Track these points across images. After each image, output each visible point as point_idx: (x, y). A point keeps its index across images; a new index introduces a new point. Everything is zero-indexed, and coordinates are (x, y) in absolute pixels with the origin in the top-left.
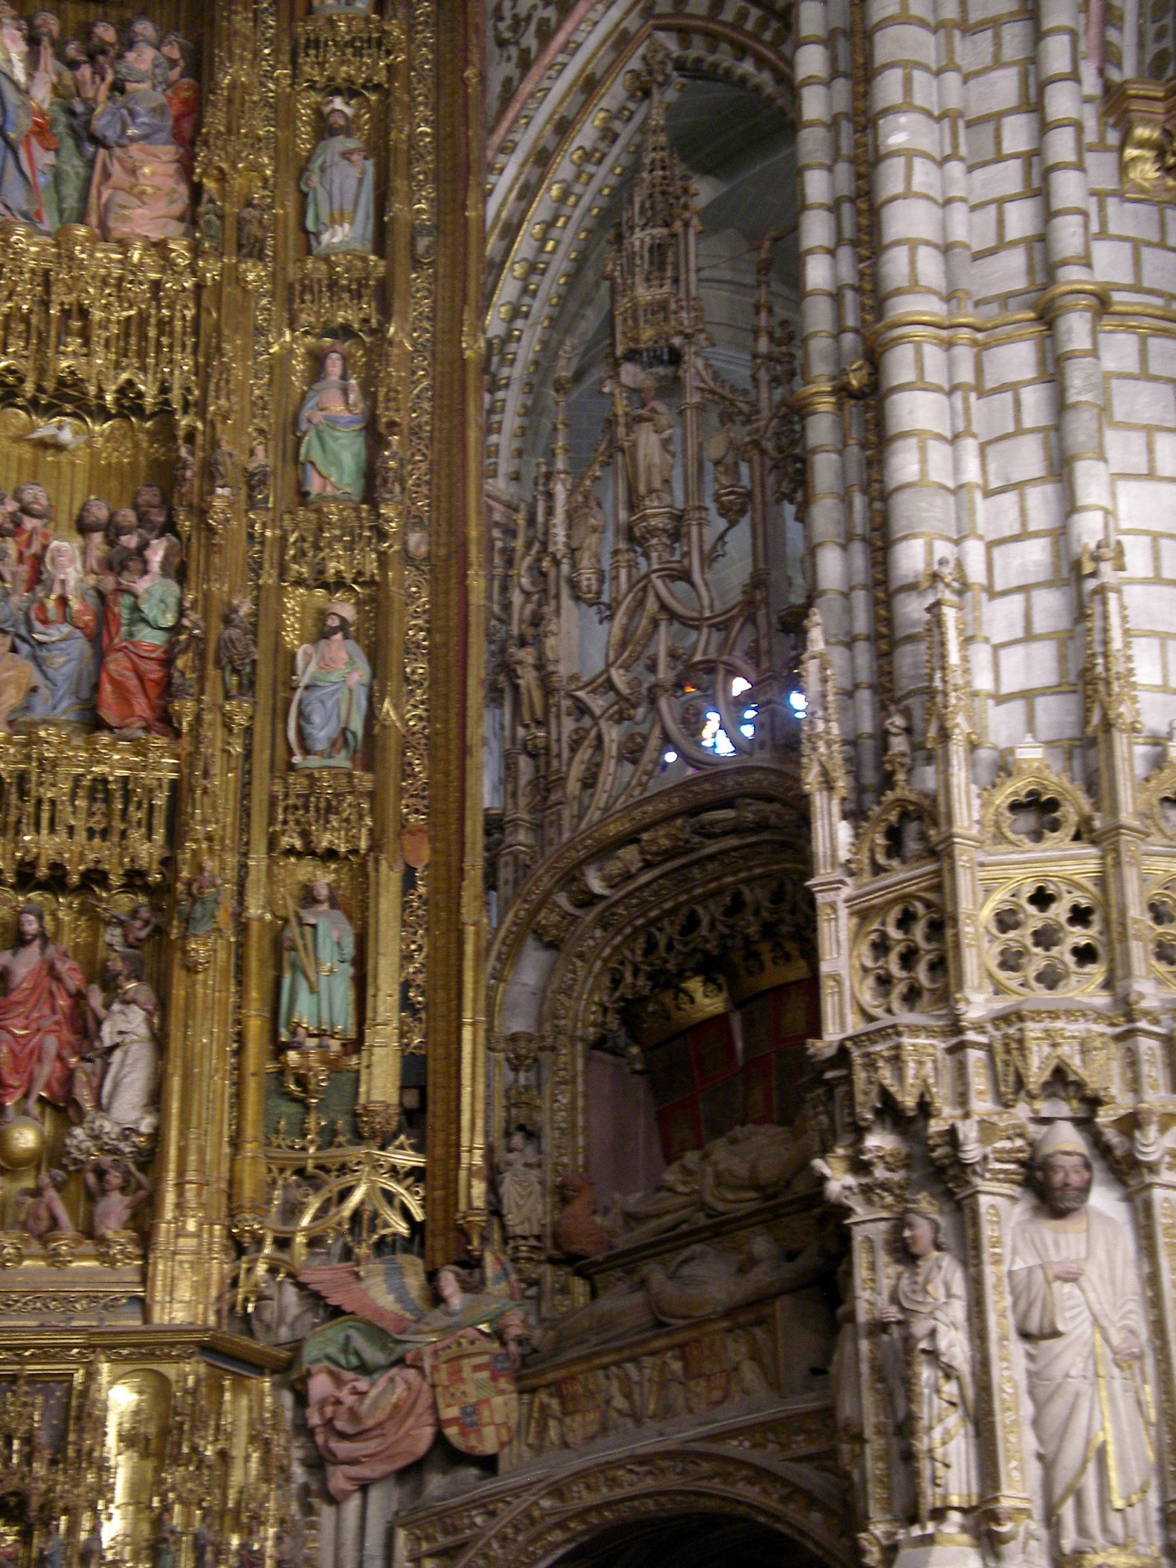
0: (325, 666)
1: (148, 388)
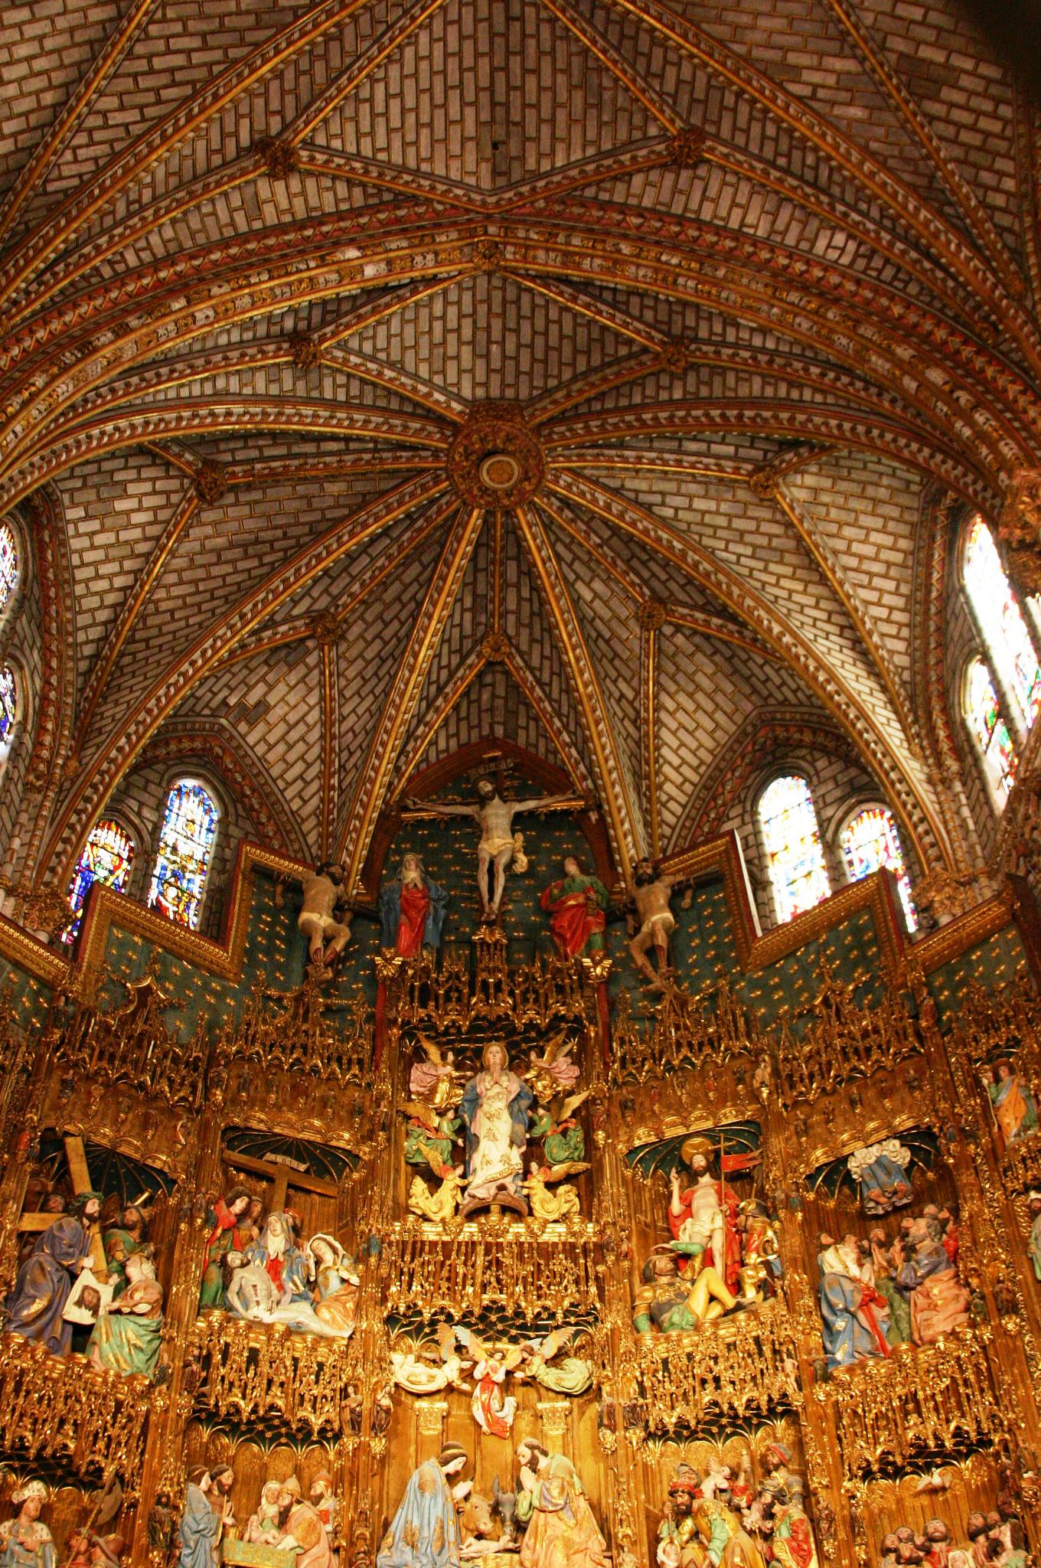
1: (969, 1427)
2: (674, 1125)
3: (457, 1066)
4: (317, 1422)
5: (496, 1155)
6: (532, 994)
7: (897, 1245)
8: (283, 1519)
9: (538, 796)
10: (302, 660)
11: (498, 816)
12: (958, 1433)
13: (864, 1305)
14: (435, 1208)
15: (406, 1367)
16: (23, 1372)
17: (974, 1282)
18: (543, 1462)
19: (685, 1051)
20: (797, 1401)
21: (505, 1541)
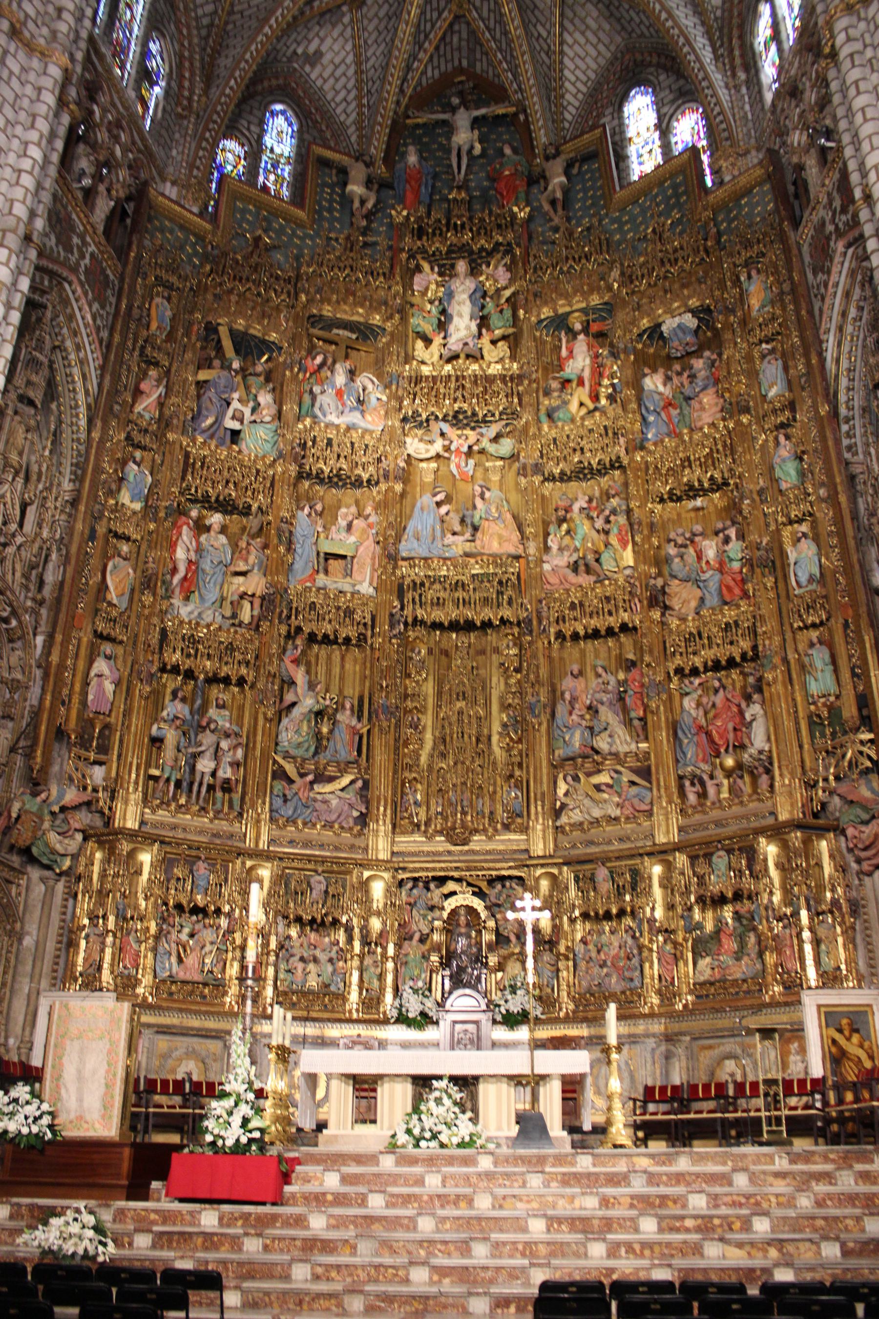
0: (799, 553)
2: (563, 306)
3: (441, 274)
4: (365, 476)
5: (463, 325)
6: (483, 230)
7: (686, 375)
8: (349, 526)
9: (487, 104)
10: (340, 20)
11: (462, 119)
12: (712, 478)
13: (665, 408)
14: (428, 358)
15: (414, 446)
16: (205, 457)
17: (727, 395)
18: (487, 495)
19: (571, 262)
20: (625, 462)
21: (468, 536)
